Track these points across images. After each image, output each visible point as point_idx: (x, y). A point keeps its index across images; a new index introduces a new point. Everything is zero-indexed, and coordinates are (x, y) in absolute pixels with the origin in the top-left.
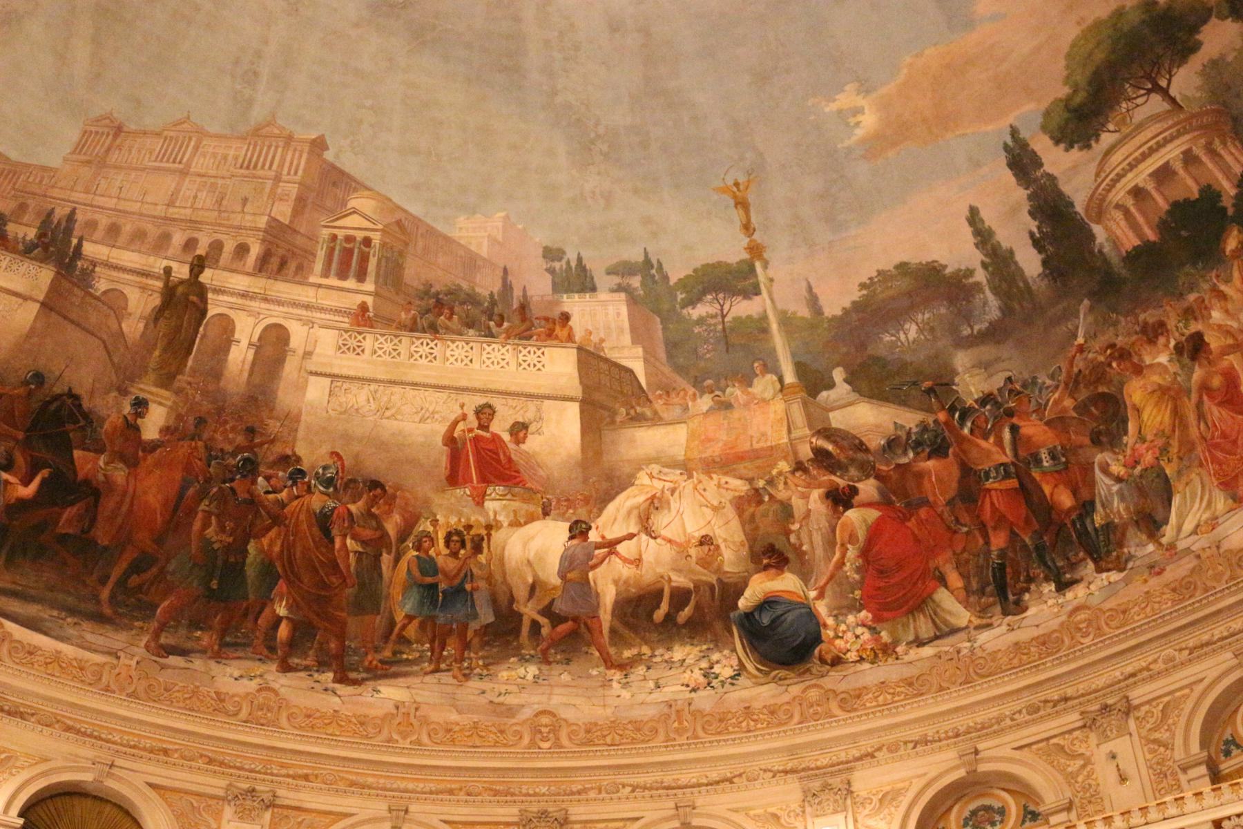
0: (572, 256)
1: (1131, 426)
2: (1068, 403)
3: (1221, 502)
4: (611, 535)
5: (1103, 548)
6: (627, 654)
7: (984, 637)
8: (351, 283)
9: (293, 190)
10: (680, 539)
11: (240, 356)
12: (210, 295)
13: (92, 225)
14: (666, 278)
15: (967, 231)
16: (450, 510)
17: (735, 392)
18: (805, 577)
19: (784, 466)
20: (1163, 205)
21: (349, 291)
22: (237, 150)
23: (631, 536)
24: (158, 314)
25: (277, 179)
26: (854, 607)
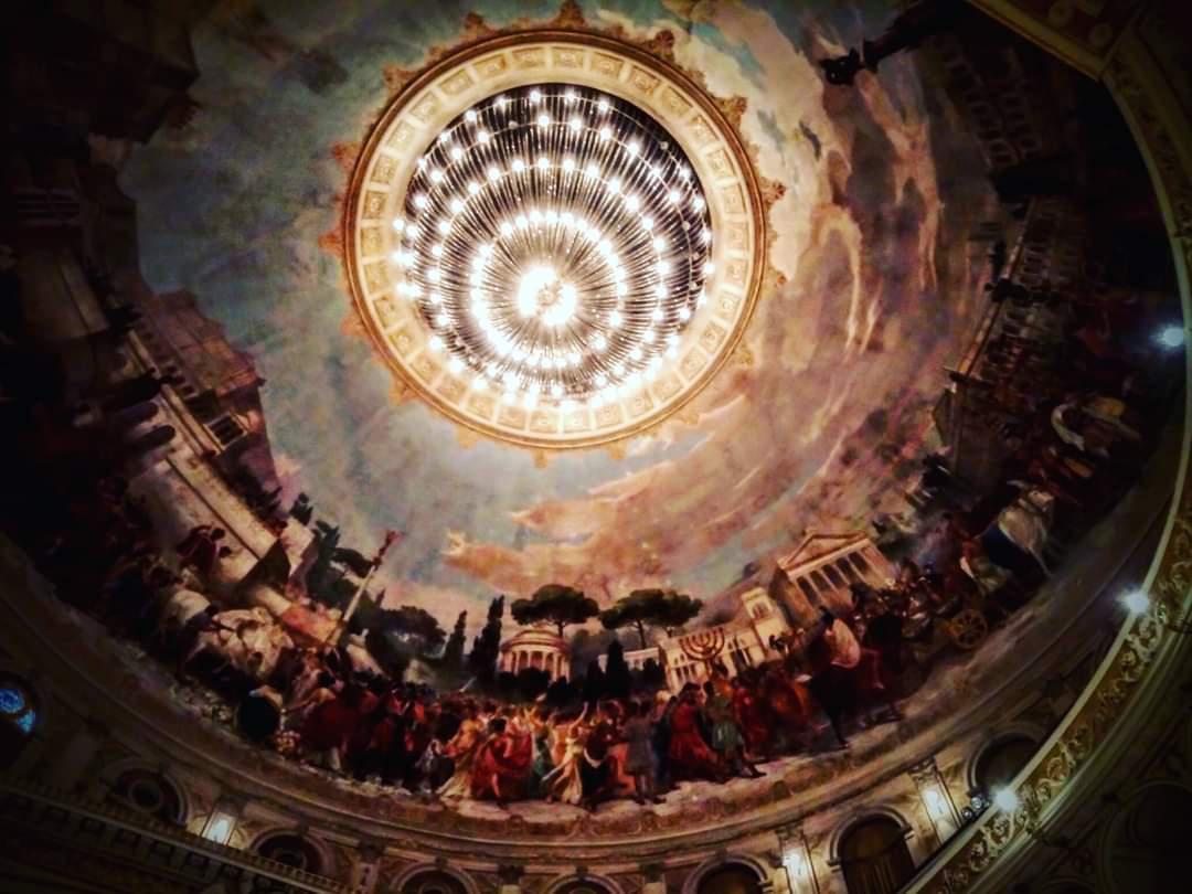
0: (310, 504)
1: (455, 738)
2: (439, 711)
3: (467, 793)
4: (224, 622)
5: (412, 782)
6: (189, 678)
7: (340, 780)
8: (218, 441)
10: (249, 646)
11: (147, 426)
12: (159, 396)
13: (143, 326)
14: (336, 543)
15: (454, 620)
16: (166, 560)
17: (321, 607)
18: (286, 702)
19: (314, 650)
20: (529, 665)
21: (215, 443)
22: (229, 355)
23: (230, 629)
24: (129, 382)
25: (231, 379)
26: (296, 730)
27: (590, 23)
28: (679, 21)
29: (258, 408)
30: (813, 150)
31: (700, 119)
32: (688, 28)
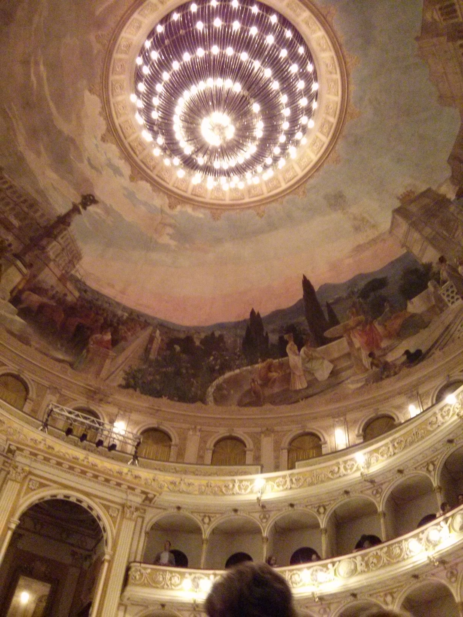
9: (435, 40)
25: (435, 45)
27: (207, 212)
28: (167, 214)
29: (424, 20)
30: (92, 162)
31: (152, 168)
32: (162, 211)
